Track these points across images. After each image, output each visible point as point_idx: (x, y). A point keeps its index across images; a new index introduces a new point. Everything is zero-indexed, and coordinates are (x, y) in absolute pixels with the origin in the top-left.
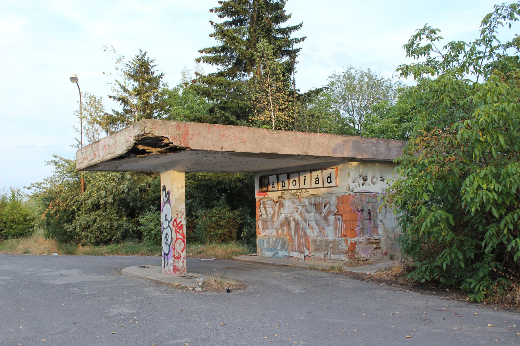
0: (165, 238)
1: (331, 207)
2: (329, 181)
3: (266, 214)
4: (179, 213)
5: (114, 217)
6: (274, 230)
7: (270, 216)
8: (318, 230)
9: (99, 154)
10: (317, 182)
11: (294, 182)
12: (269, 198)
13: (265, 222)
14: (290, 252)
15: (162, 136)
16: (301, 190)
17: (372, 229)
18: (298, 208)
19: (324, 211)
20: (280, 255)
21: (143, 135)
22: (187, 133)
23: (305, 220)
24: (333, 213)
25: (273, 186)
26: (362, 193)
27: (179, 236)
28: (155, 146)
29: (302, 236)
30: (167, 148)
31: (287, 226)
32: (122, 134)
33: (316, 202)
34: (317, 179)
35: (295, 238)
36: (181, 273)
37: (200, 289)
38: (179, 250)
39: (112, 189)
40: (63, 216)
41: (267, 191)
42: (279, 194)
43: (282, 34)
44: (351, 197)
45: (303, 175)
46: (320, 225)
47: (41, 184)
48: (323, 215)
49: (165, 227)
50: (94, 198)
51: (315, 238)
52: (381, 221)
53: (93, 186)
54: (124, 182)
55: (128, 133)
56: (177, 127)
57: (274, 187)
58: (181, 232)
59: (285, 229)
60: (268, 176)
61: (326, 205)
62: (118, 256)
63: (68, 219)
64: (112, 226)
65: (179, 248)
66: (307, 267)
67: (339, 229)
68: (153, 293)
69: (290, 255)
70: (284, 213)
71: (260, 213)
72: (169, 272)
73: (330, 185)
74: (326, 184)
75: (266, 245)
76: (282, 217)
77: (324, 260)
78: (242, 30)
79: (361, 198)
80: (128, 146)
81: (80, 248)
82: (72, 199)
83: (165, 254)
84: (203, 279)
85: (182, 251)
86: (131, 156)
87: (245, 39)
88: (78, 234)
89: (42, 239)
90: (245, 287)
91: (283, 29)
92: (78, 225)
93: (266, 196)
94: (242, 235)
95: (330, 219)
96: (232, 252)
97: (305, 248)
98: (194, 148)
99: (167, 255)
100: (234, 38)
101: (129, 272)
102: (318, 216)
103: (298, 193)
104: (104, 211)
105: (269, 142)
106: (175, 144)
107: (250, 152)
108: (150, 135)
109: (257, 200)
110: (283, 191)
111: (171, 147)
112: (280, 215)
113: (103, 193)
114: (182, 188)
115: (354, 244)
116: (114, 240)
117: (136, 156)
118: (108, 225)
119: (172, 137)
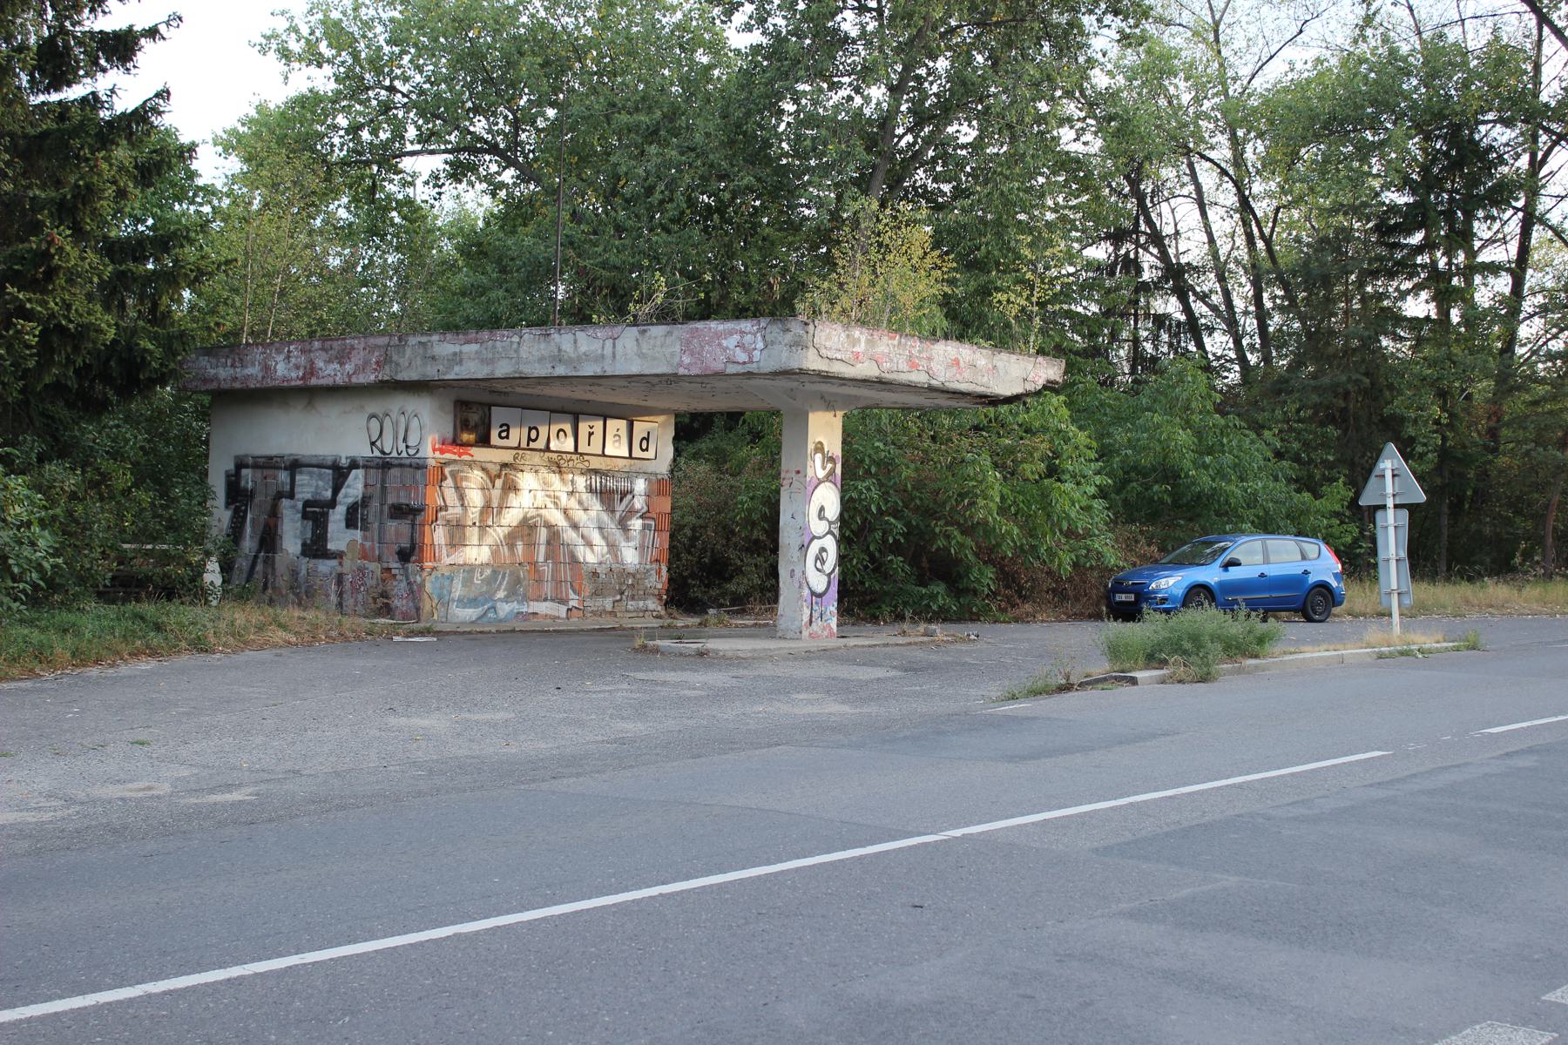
0: (817, 558)
3: (462, 505)
7: (473, 514)
11: (561, 433)
18: (557, 498)
19: (620, 508)
20: (502, 614)
23: (575, 526)
25: (504, 434)
35: (547, 570)
45: (585, 420)
59: (520, 547)
60: (490, 406)
69: (531, 611)
76: (511, 517)
77: (613, 613)
83: (813, 593)
99: (820, 596)
102: (605, 517)
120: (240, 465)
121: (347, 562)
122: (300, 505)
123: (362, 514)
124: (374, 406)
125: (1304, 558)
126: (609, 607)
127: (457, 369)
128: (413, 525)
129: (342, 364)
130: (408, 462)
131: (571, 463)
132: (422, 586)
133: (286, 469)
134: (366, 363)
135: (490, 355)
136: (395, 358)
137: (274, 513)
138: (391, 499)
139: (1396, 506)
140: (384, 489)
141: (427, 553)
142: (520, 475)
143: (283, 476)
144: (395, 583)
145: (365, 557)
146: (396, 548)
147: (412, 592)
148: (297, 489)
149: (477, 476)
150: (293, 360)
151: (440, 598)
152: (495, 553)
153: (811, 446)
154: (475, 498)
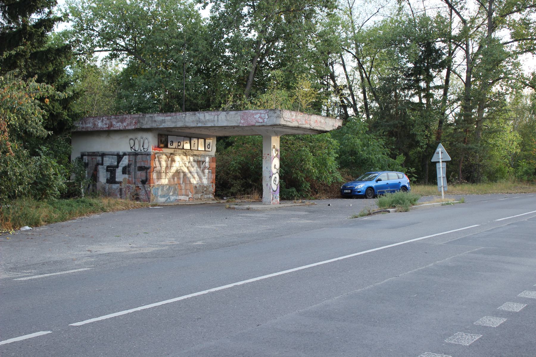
7: (163, 169)
13: (159, 173)
18: (186, 164)
19: (202, 166)
20: (171, 200)
23: (190, 172)
60: (168, 135)
70: (176, 166)
75: (160, 194)
76: (173, 170)
77: (201, 199)
83: (273, 191)
93: (161, 152)
99: (275, 191)
102: (199, 170)
120: (83, 155)
121: (123, 185)
122: (105, 167)
123: (128, 170)
124: (131, 136)
125: (399, 178)
126: (200, 198)
127: (163, 124)
128: (146, 173)
129: (122, 123)
130: (144, 153)
132: (150, 191)
133: (100, 156)
134: (131, 123)
135: (175, 120)
136: (141, 121)
137: (96, 170)
138: (138, 165)
139: (442, 162)
140: (135, 162)
141: (151, 181)
142: (175, 157)
143: (99, 159)
144: (140, 191)
145: (129, 182)
146: (141, 180)
147: (147, 193)
148: (104, 162)
149: (164, 157)
150: (104, 122)
151: (155, 195)
152: (169, 181)
153: (272, 147)
154: (164, 164)
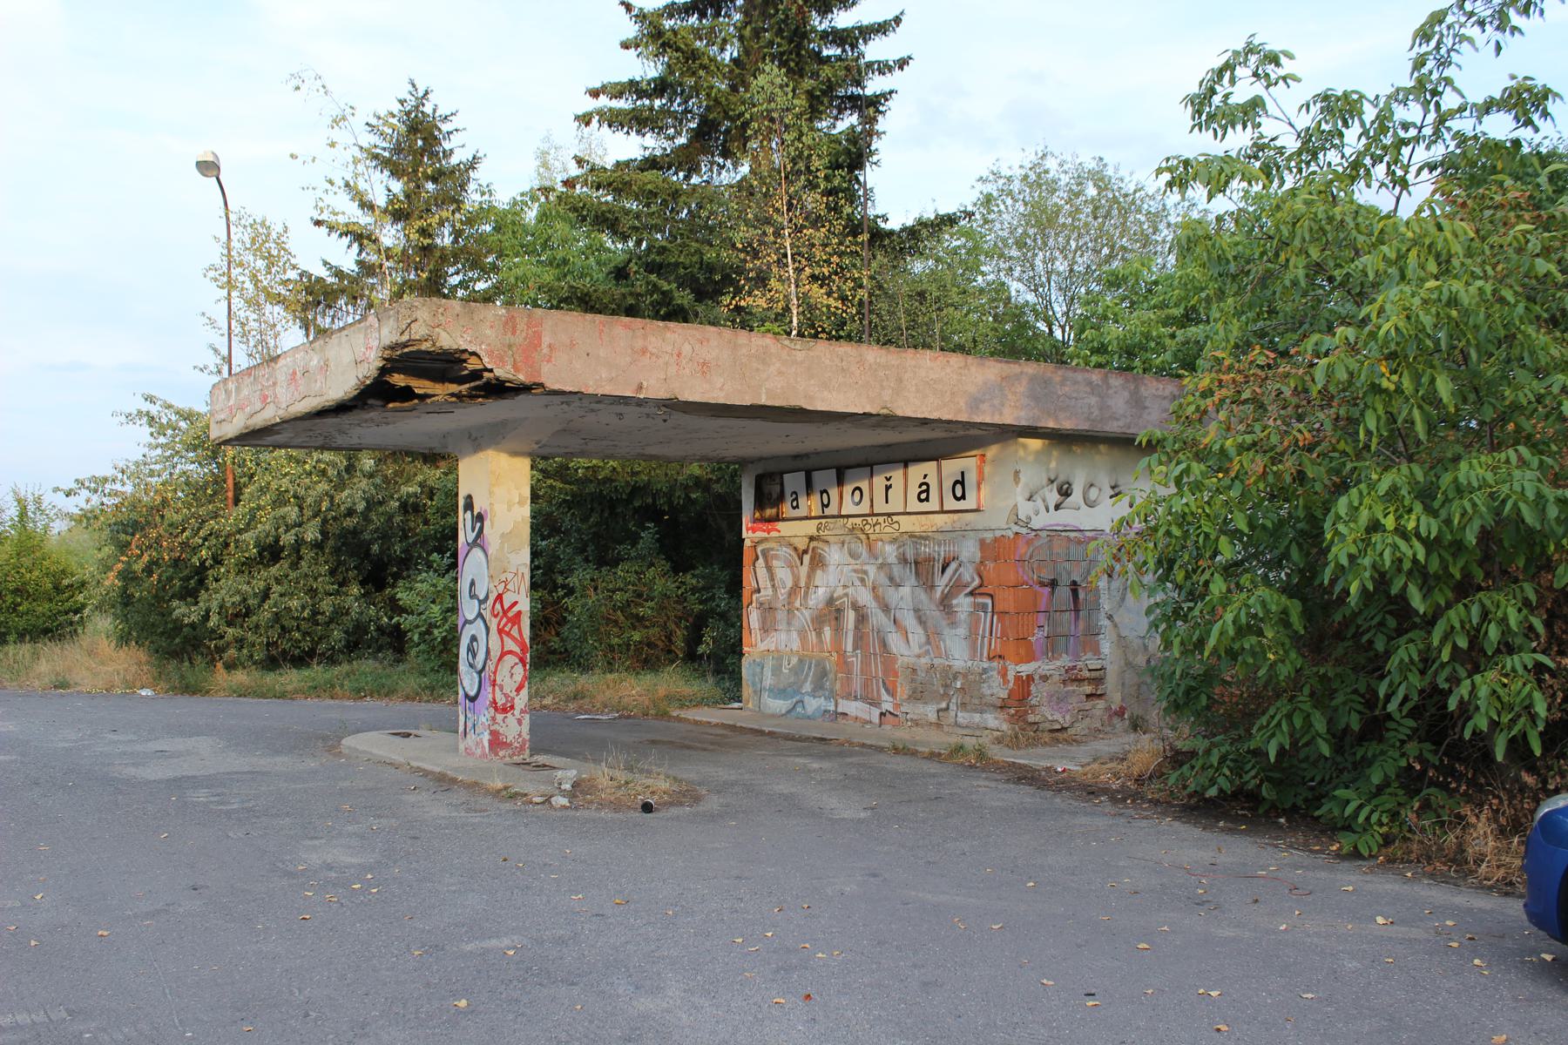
0: (469, 650)
1: (962, 569)
2: (959, 494)
3: (773, 586)
4: (510, 576)
5: (324, 584)
6: (795, 635)
7: (783, 593)
8: (923, 639)
9: (276, 397)
10: (923, 496)
11: (857, 492)
12: (781, 540)
13: (768, 610)
14: (840, 701)
15: (463, 348)
16: (875, 519)
17: (1082, 638)
18: (865, 572)
19: (942, 582)
21: (405, 345)
22: (535, 342)
23: (886, 608)
24: (969, 590)
26: (1054, 533)
27: (511, 645)
28: (441, 377)
29: (875, 654)
30: (477, 383)
31: (833, 623)
32: (344, 339)
33: (917, 554)
34: (924, 487)
35: (856, 661)
36: (514, 754)
37: (564, 801)
38: (510, 686)
39: (319, 502)
40: (170, 579)
41: (777, 518)
42: (810, 527)
43: (838, 46)
44: (1021, 543)
45: (880, 473)
46: (929, 624)
47: (106, 480)
48: (938, 593)
49: (470, 617)
50: (264, 527)
51: (913, 660)
52: (1110, 617)
53: (263, 491)
54: (355, 480)
55: (362, 336)
56: (506, 323)
57: (797, 507)
58: (515, 632)
59: (827, 632)
60: (782, 473)
61: (948, 565)
62: (332, 702)
63: (186, 587)
64: (315, 613)
65: (507, 679)
66: (887, 745)
67: (983, 637)
68: (427, 809)
69: (840, 710)
70: (826, 584)
71: (754, 584)
72: (479, 751)
73: (961, 505)
74: (951, 504)
75: (768, 680)
76: (818, 596)
77: (939, 725)
78: (720, 31)
79: (1050, 548)
80: (360, 376)
81: (221, 675)
82: (199, 529)
83: (467, 696)
84: (574, 772)
85: (519, 689)
86: (372, 406)
87: (728, 58)
88: (215, 634)
89: (106, 647)
90: (697, 799)
91: (844, 30)
92: (215, 606)
93: (774, 534)
94: (702, 649)
95: (957, 605)
96: (669, 698)
97: (883, 691)
98: (556, 387)
100: (693, 55)
101: (361, 748)
102: (923, 596)
103: (867, 527)
104: (295, 566)
105: (780, 373)
106: (500, 373)
107: (721, 401)
108: (425, 346)
109: (747, 543)
110: (823, 521)
111: (488, 383)
112: (812, 589)
113: (292, 512)
114: (521, 503)
115: (1025, 683)
116: (323, 654)
117: (384, 406)
118: (303, 608)
119: (490, 353)
131: (877, 527)
